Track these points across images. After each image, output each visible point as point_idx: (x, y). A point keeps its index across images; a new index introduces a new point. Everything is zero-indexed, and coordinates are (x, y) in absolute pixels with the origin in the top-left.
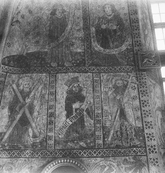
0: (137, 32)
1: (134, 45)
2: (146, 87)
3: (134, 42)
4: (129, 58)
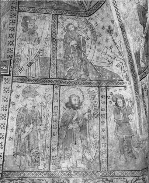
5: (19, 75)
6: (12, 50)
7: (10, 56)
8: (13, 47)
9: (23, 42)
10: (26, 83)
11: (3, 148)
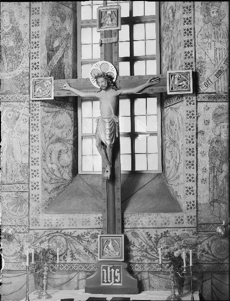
0: (36, 50)
1: (31, 67)
2: (38, 120)
3: (31, 64)
4: (24, 85)
5: (206, 91)
6: (191, 55)
7: (189, 64)
8: (192, 49)
9: (206, 40)
10: (216, 102)
11: (195, 194)
